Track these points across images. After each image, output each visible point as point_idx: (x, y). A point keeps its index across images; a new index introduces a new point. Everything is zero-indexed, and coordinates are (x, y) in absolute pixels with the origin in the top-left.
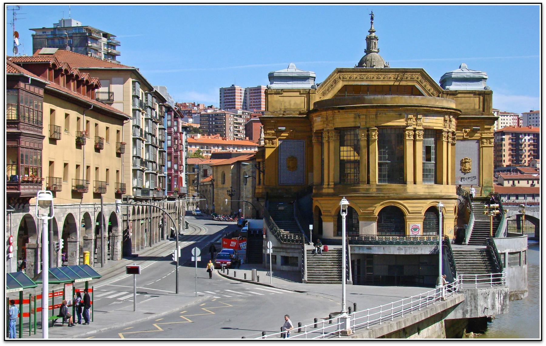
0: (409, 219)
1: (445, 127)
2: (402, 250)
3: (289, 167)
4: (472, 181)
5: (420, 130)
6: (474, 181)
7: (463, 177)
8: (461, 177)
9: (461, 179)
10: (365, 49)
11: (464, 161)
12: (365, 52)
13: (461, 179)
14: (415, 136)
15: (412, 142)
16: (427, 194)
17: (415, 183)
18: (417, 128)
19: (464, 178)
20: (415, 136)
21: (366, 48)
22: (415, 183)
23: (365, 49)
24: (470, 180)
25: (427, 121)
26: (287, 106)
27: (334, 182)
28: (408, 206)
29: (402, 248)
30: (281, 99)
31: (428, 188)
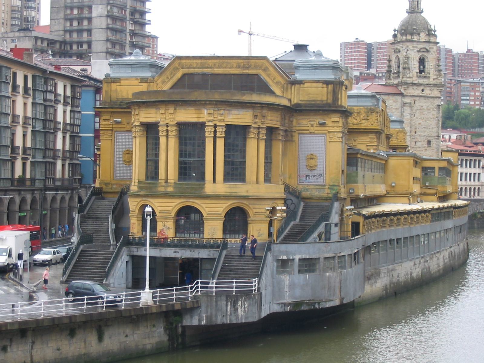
0: (207, 220)
1: (255, 123)
2: (178, 253)
3: (124, 161)
4: (317, 179)
5: (222, 126)
6: (320, 179)
7: (308, 174)
8: (306, 174)
9: (306, 176)
10: (407, 10)
11: (309, 157)
12: (407, 12)
13: (306, 176)
14: (215, 132)
15: (212, 140)
16: (229, 194)
17: (214, 181)
18: (218, 124)
19: (309, 176)
20: (215, 132)
21: (408, 8)
22: (214, 181)
23: (407, 10)
24: (315, 178)
25: (231, 116)
26: (124, 96)
27: (138, 179)
28: (204, 207)
29: (178, 251)
30: (119, 88)
31: (230, 188)
